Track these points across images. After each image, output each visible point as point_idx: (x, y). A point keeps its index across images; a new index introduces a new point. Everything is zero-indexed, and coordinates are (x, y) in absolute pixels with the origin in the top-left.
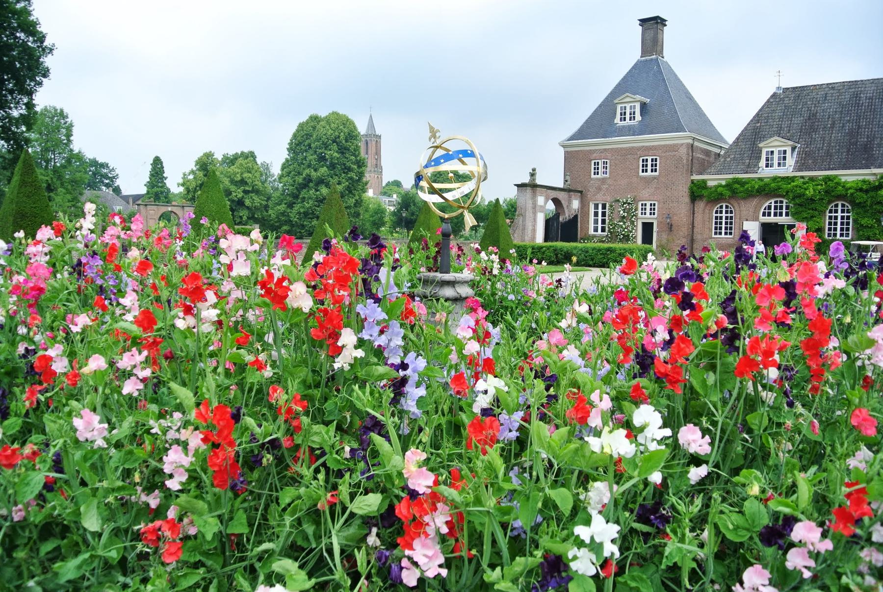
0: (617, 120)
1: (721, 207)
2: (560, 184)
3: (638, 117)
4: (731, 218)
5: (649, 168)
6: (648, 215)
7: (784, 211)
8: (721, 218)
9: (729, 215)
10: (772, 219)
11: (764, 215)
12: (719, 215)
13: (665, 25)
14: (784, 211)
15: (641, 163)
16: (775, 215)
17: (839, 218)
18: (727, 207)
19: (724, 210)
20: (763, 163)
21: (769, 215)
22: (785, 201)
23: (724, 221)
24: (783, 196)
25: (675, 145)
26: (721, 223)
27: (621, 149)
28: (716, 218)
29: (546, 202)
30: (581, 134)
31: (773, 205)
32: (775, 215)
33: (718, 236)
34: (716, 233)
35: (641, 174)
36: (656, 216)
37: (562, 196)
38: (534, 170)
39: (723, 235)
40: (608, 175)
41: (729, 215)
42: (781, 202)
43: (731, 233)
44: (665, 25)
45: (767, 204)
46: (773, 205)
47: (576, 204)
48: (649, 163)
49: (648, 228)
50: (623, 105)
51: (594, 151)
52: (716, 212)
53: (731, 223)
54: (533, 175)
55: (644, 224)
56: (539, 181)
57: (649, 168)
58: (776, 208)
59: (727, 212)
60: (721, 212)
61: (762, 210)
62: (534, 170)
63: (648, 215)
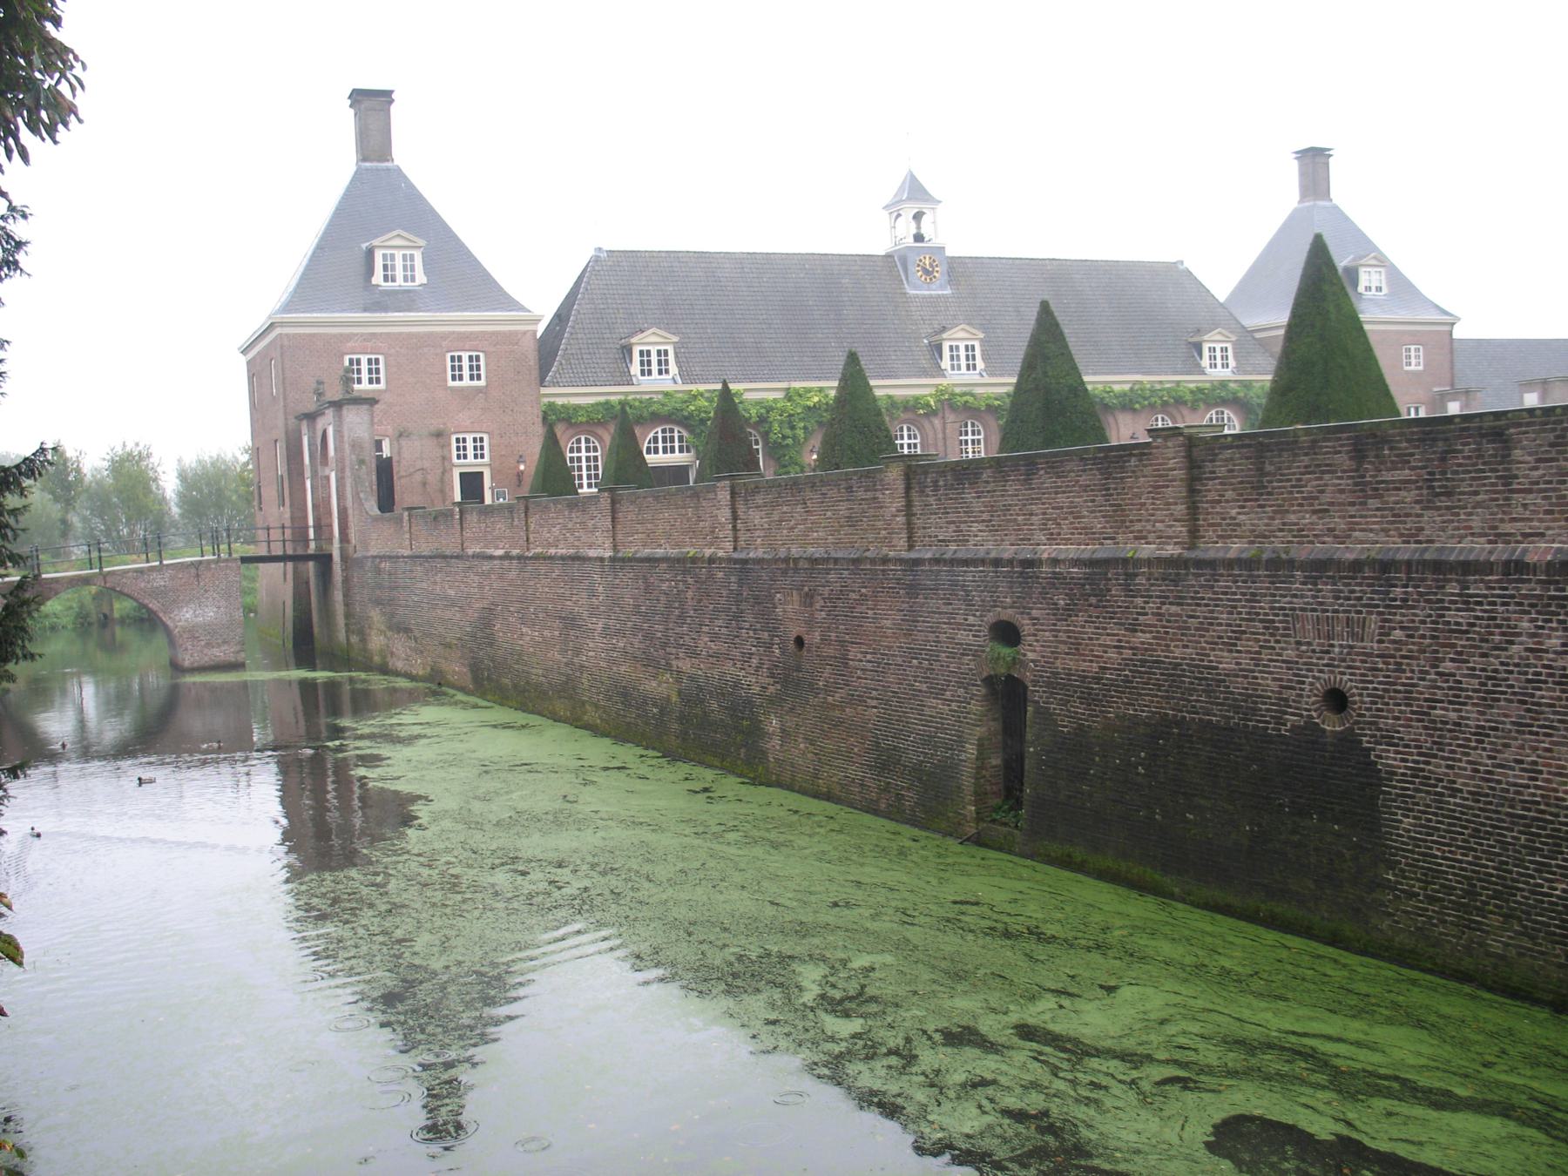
0: (378, 278)
1: (579, 441)
3: (421, 278)
5: (466, 372)
6: (470, 458)
7: (677, 444)
14: (677, 444)
15: (449, 364)
17: (584, 459)
18: (587, 441)
19: (583, 445)
20: (635, 368)
21: (656, 451)
23: (584, 464)
24: (679, 423)
25: (511, 333)
27: (410, 335)
32: (665, 451)
35: (451, 383)
36: (487, 459)
40: (382, 386)
42: (672, 431)
45: (651, 435)
48: (466, 364)
50: (389, 252)
51: (349, 337)
55: (461, 474)
57: (466, 372)
58: (664, 440)
59: (588, 450)
60: (579, 450)
61: (646, 445)
63: (470, 458)
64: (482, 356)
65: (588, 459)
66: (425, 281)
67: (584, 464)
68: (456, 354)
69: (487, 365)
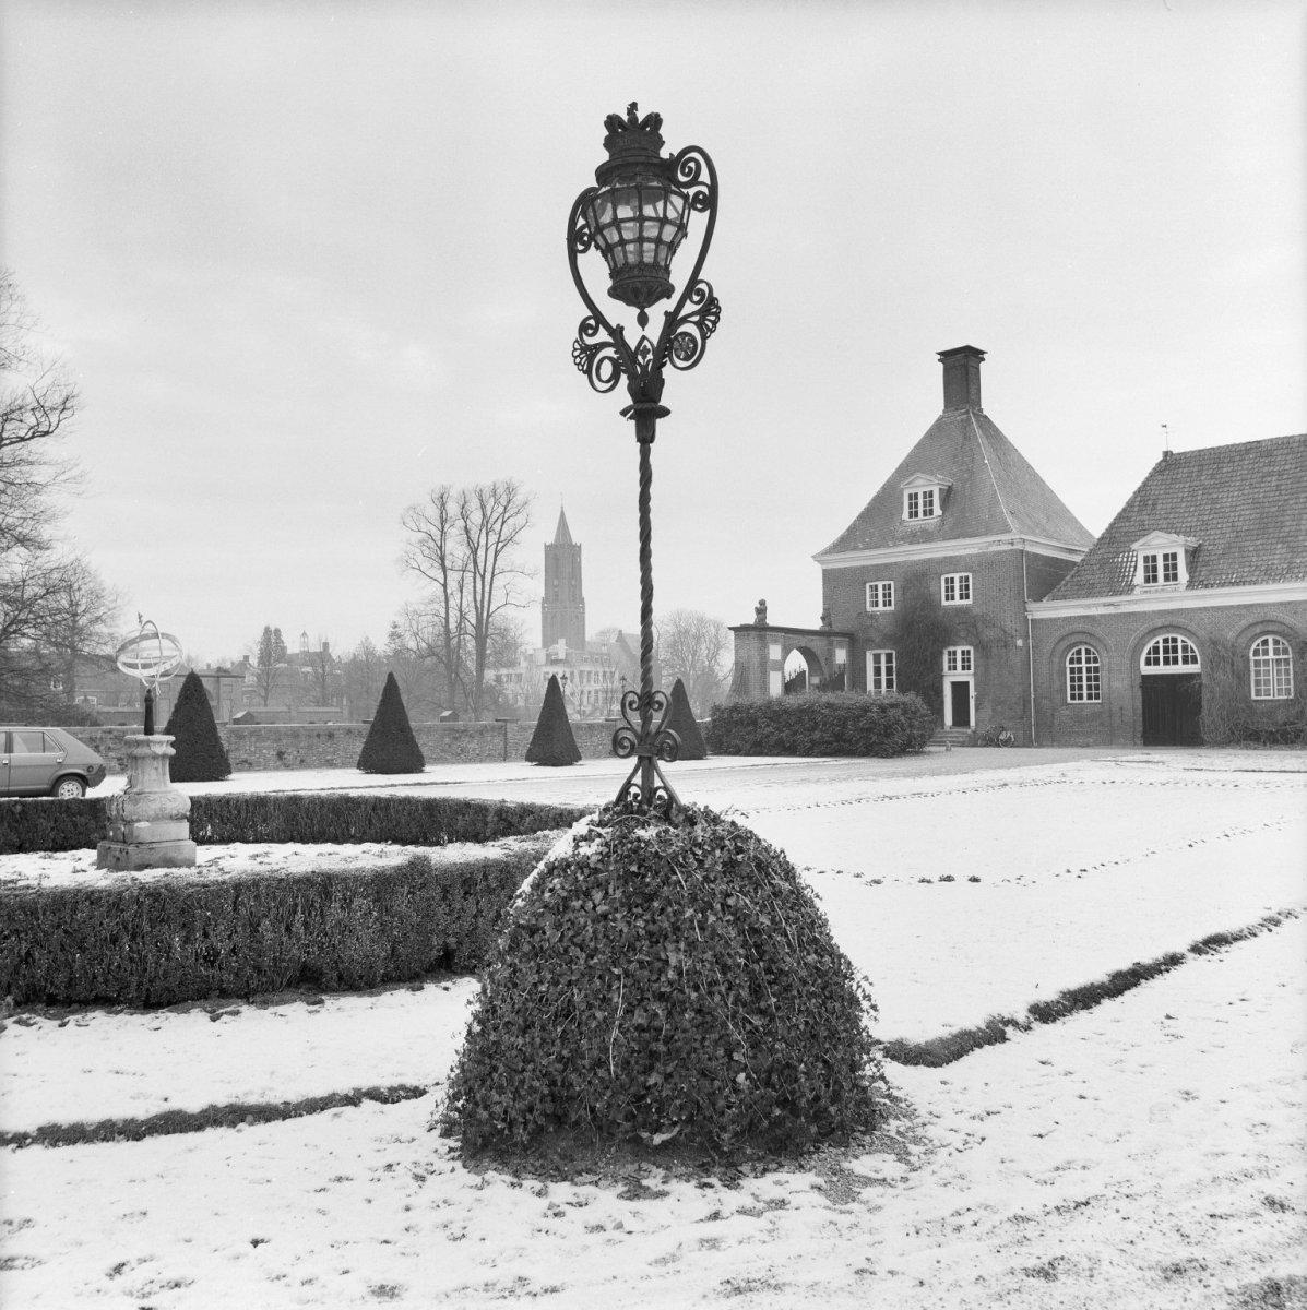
2: (817, 625)
3: (937, 511)
4: (1096, 669)
5: (957, 593)
7: (1180, 655)
8: (1080, 670)
9: (1092, 665)
10: (1161, 669)
11: (1148, 662)
12: (1076, 666)
13: (983, 360)
14: (1180, 655)
16: (1166, 662)
18: (1088, 652)
19: (1083, 656)
22: (1180, 638)
23: (1084, 675)
26: (1080, 679)
28: (1072, 670)
29: (786, 652)
30: (845, 543)
31: (1161, 646)
33: (1077, 701)
34: (1073, 697)
37: (817, 645)
38: (762, 603)
39: (1085, 700)
41: (1092, 665)
43: (1097, 697)
44: (983, 360)
45: (1151, 645)
46: (1161, 646)
47: (841, 656)
49: (960, 689)
52: (1072, 661)
53: (1097, 679)
54: (761, 610)
56: (771, 621)
58: (1166, 650)
60: (1079, 661)
62: (762, 603)
64: (970, 575)
65: (1089, 670)
66: (940, 513)
67: (1084, 675)
68: (949, 576)
69: (973, 584)
